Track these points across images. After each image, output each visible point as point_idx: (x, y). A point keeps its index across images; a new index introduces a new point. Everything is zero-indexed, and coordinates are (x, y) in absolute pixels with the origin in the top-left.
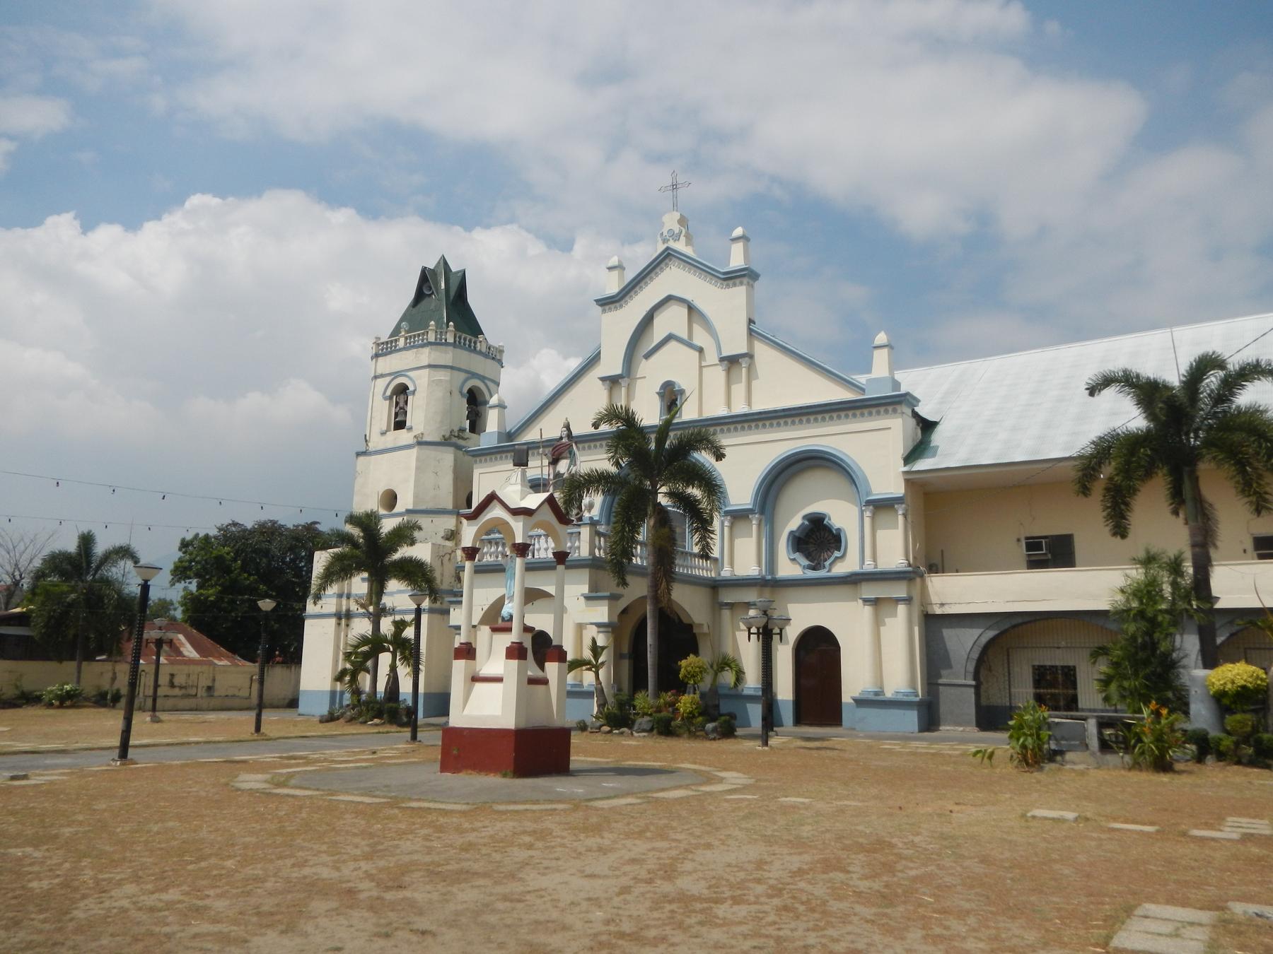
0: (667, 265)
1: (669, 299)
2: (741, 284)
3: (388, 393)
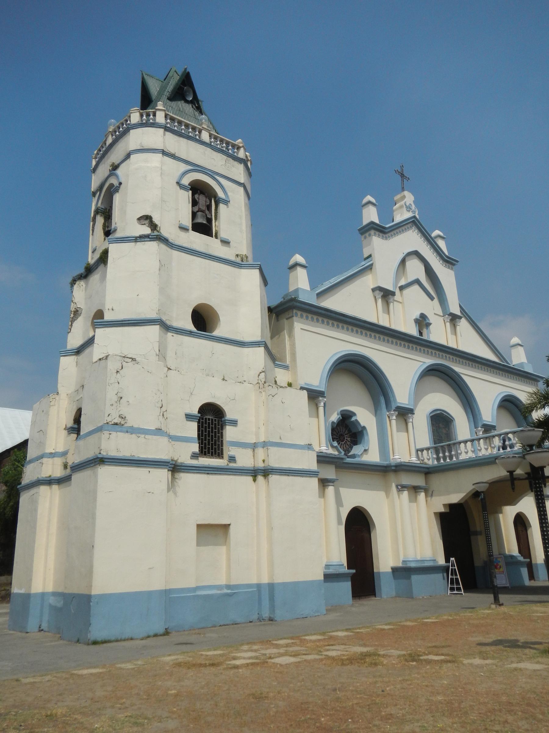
0: (411, 227)
1: (416, 254)
2: (452, 269)
3: (186, 181)
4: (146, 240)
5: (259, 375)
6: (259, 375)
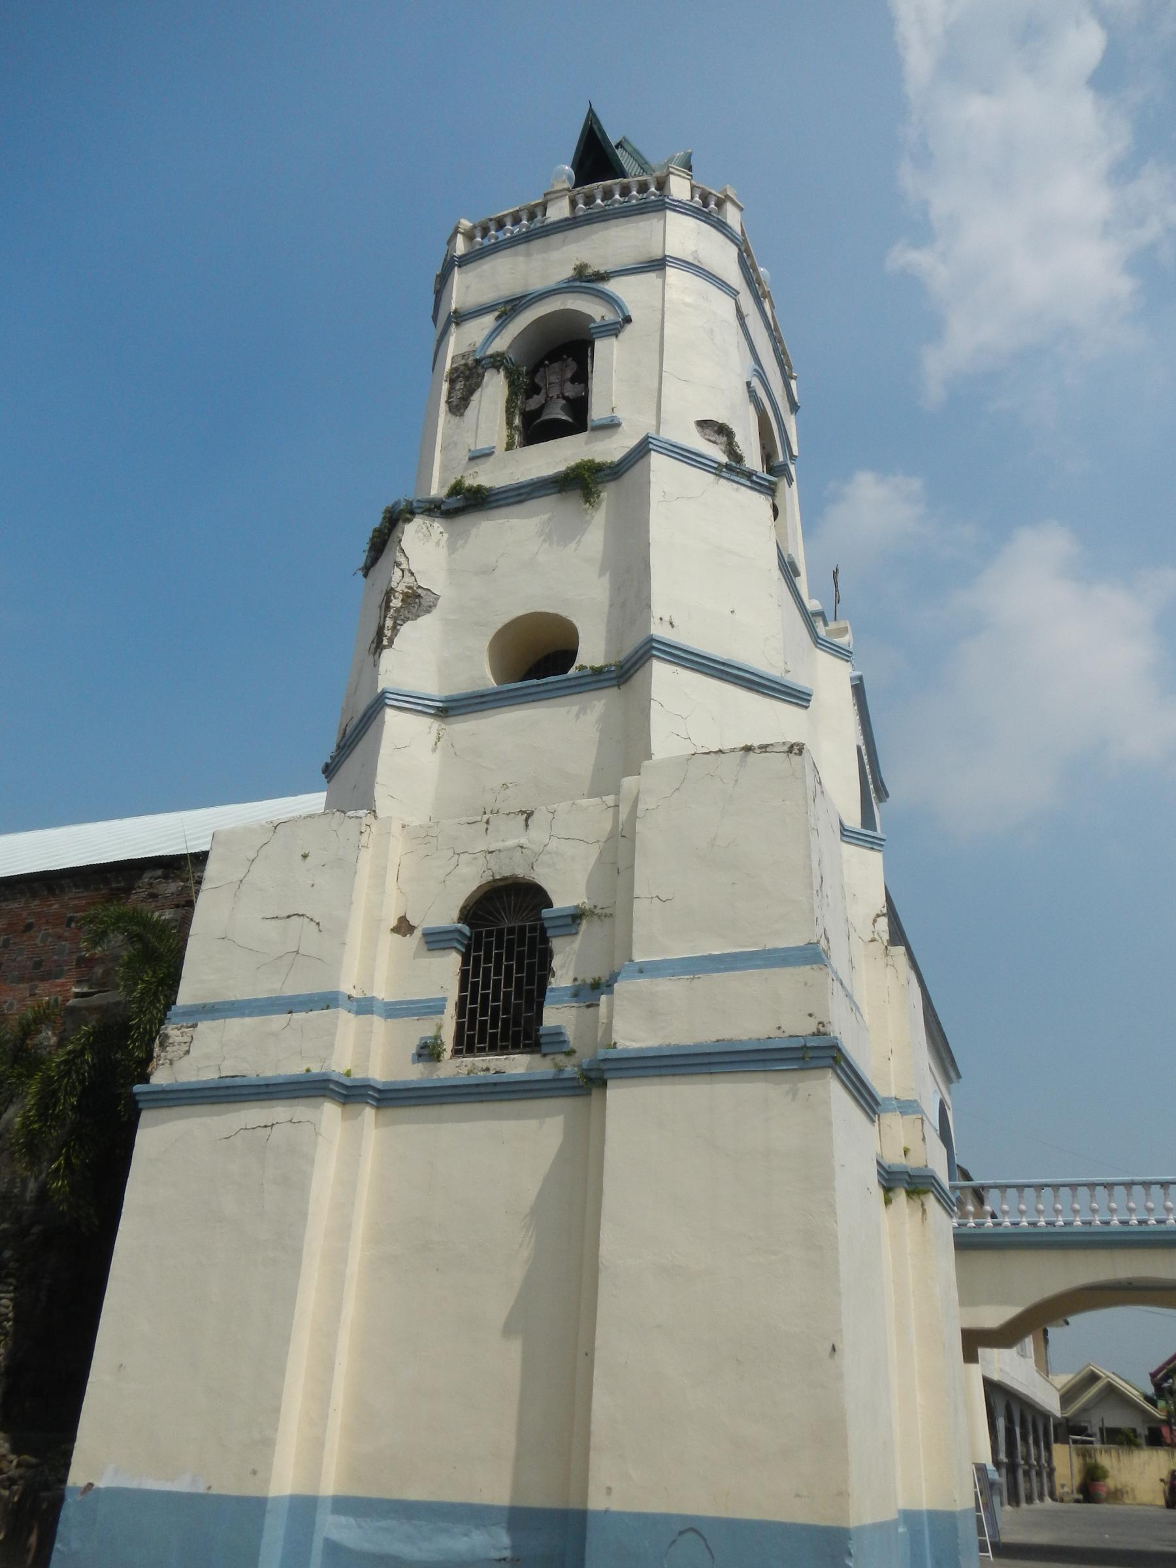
4: (743, 481)
5: (875, 921)
6: (875, 921)
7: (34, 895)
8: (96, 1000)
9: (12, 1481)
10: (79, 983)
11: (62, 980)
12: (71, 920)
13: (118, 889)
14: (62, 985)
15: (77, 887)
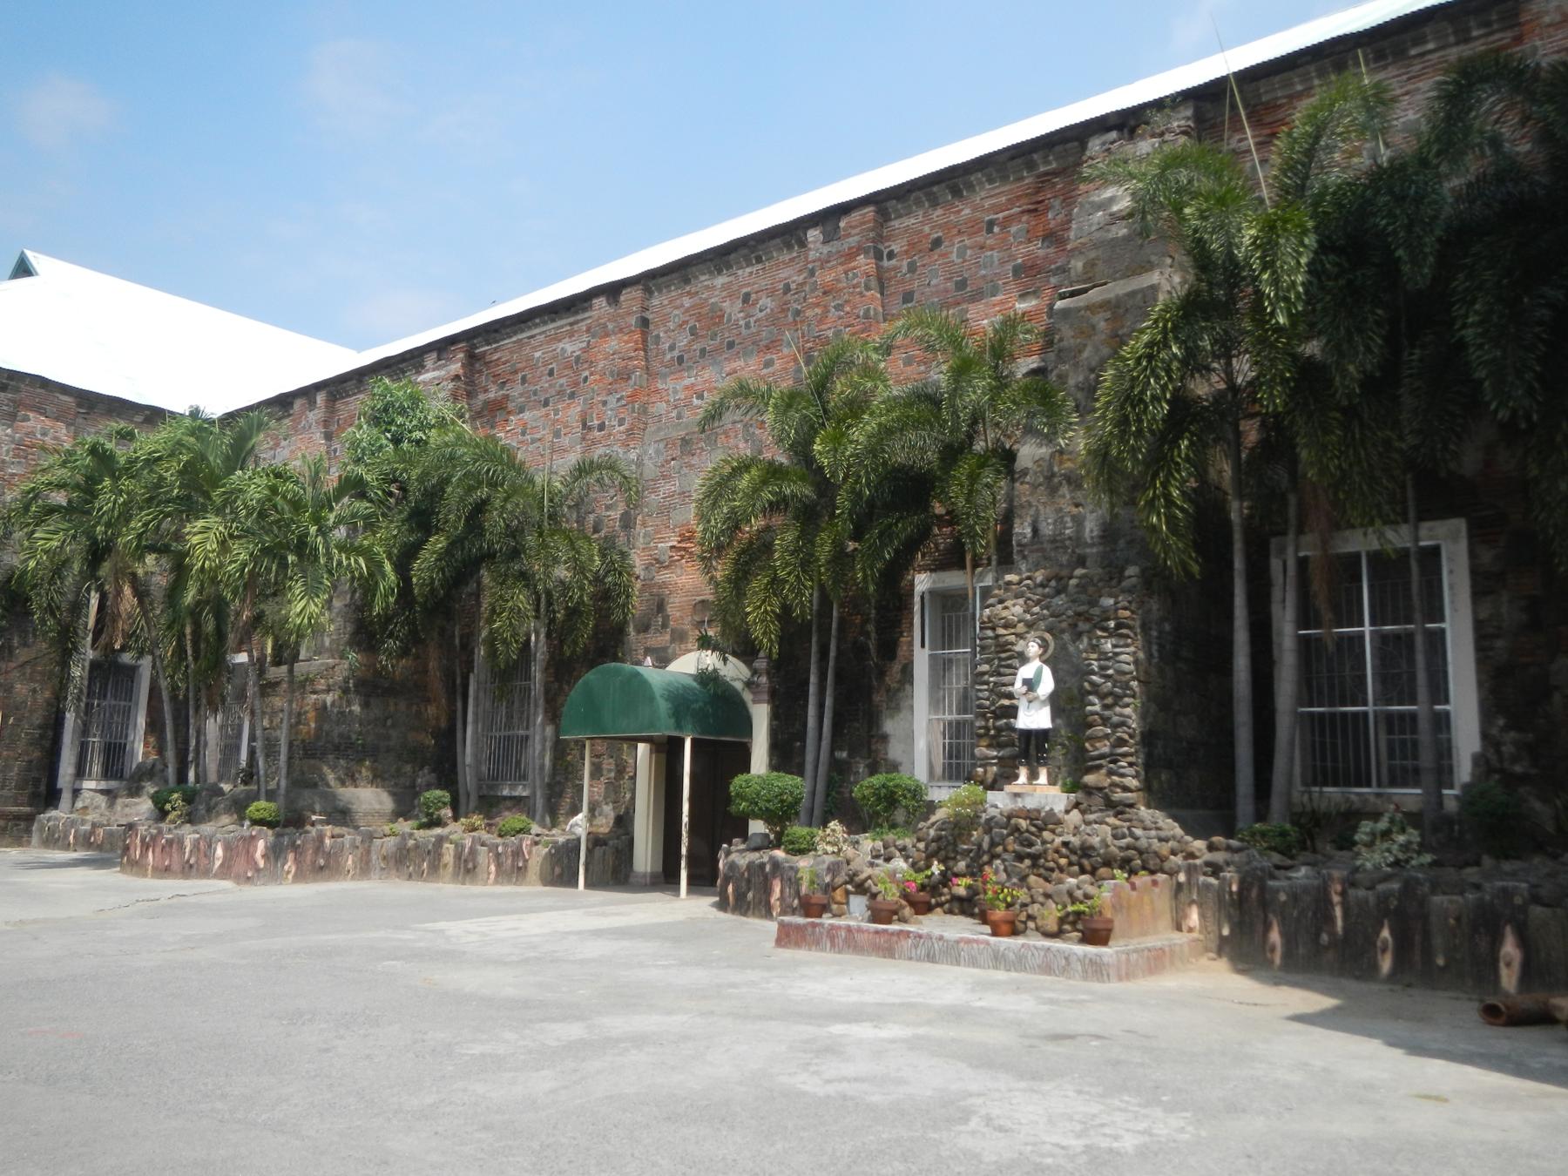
7: (935, 204)
8: (1095, 295)
9: (1215, 869)
10: (1023, 296)
11: (999, 297)
12: (991, 224)
13: (1046, 174)
14: (1002, 303)
15: (991, 181)
